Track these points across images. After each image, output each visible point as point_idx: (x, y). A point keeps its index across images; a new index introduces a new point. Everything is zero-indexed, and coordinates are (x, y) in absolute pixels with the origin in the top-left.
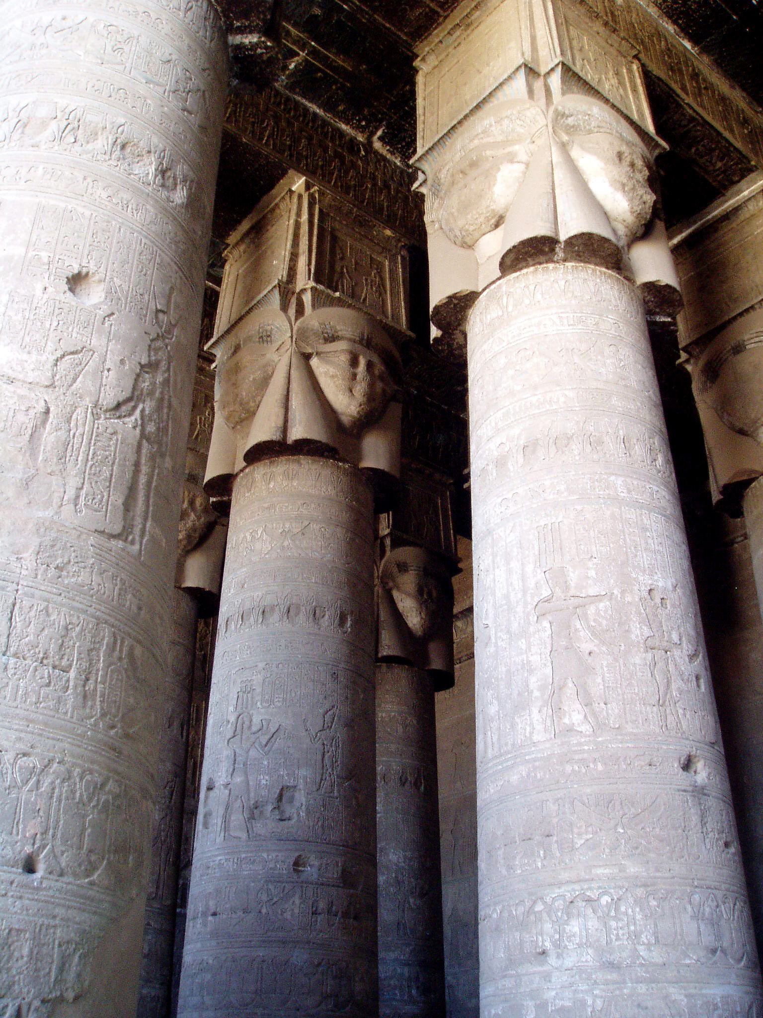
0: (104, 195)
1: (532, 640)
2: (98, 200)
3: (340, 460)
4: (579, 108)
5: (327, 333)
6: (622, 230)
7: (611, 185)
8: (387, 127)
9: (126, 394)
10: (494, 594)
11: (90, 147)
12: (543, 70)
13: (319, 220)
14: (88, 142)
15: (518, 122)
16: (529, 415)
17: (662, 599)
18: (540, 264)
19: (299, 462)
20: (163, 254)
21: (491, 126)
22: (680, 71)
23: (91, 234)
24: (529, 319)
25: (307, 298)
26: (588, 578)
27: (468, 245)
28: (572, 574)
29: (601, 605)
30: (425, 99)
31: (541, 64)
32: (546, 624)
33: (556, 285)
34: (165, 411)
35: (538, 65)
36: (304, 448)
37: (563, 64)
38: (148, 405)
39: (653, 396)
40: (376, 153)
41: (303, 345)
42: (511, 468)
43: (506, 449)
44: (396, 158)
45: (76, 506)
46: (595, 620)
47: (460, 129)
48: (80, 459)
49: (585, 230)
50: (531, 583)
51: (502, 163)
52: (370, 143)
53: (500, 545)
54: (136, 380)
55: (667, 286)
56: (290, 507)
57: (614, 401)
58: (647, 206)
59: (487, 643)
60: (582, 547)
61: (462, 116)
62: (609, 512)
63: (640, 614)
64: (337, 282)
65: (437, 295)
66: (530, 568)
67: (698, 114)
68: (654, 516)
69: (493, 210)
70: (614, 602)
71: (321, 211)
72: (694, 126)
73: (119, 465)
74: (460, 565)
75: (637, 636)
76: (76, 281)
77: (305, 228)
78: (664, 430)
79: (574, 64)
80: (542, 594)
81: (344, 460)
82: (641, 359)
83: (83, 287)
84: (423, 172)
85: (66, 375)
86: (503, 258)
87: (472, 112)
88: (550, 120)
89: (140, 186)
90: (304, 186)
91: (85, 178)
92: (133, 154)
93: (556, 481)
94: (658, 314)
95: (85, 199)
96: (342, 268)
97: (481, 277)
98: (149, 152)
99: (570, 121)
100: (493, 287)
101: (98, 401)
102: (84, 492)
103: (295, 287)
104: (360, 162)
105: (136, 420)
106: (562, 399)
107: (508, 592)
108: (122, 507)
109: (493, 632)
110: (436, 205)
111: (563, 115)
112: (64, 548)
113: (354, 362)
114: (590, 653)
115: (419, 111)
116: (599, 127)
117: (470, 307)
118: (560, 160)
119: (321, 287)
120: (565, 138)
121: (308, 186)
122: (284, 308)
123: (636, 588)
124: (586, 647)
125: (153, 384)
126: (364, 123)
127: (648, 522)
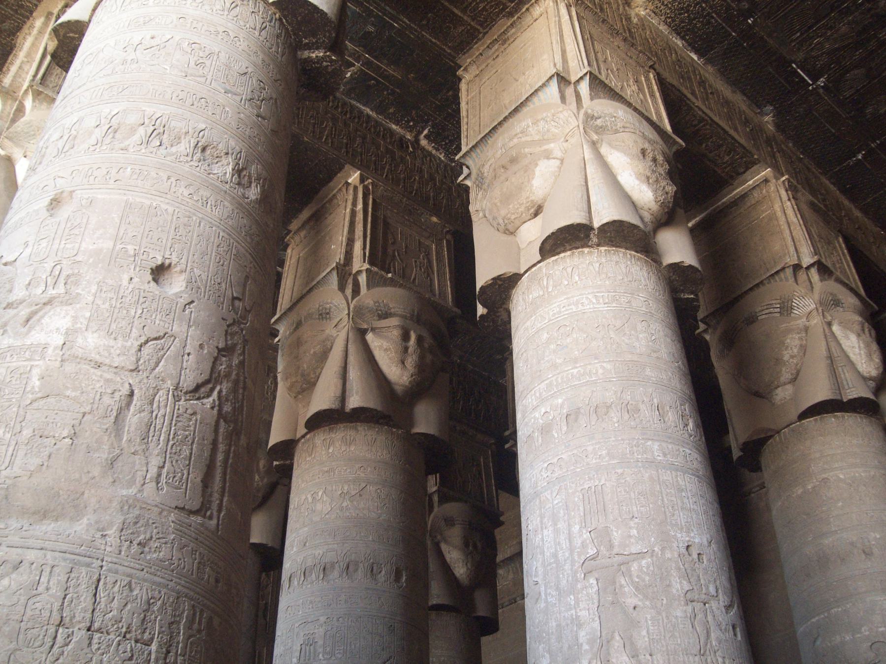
0: (186, 193)
1: (580, 596)
2: (181, 197)
3: (394, 426)
4: (606, 112)
5: (381, 310)
6: (648, 217)
7: (637, 179)
8: (433, 127)
9: (205, 376)
10: (543, 553)
11: (174, 149)
12: (573, 79)
13: (372, 209)
14: (172, 146)
15: (552, 122)
16: (571, 386)
17: (699, 554)
18: (577, 248)
19: (356, 429)
20: (239, 246)
21: (528, 127)
22: (689, 78)
23: (173, 228)
24: (568, 298)
25: (363, 279)
26: (630, 536)
28: (615, 533)
29: (644, 562)
30: (468, 104)
31: (571, 73)
32: (593, 581)
33: (591, 268)
34: (241, 391)
35: (569, 75)
36: (360, 416)
37: (591, 73)
38: (225, 387)
39: (682, 366)
40: (423, 149)
41: (359, 321)
42: (556, 435)
43: (551, 418)
44: (441, 154)
45: (158, 483)
46: (638, 577)
47: (500, 130)
48: (162, 439)
49: (616, 218)
50: (578, 542)
51: (539, 159)
52: (417, 141)
53: (547, 507)
54: (214, 363)
55: (690, 266)
56: (348, 470)
57: (648, 372)
58: (669, 195)
59: (537, 599)
60: (624, 508)
61: (502, 118)
62: (647, 475)
63: (679, 569)
64: (390, 264)
65: (483, 276)
66: (576, 528)
68: (687, 477)
69: (532, 201)
70: (655, 559)
71: (374, 200)
72: (704, 125)
73: (198, 444)
74: (501, 518)
75: (678, 591)
76: (159, 272)
77: (360, 217)
78: (693, 397)
79: (600, 73)
80: (588, 553)
81: (398, 427)
82: (669, 332)
83: (166, 277)
84: (468, 167)
85: (149, 360)
89: (218, 184)
90: (359, 178)
91: (169, 178)
92: (213, 156)
93: (597, 446)
94: (683, 291)
95: (168, 196)
96: (394, 251)
97: (522, 260)
98: (227, 154)
99: (599, 122)
100: (533, 269)
101: (179, 383)
102: (165, 471)
103: (351, 269)
104: (408, 157)
105: (214, 400)
106: (600, 371)
107: (556, 550)
108: (201, 484)
109: (543, 589)
111: (593, 117)
112: (147, 525)
113: (405, 337)
114: (635, 608)
115: (463, 113)
116: (624, 127)
117: (514, 287)
118: (592, 156)
119: (375, 269)
120: (595, 137)
121: (362, 179)
122: (342, 288)
123: (675, 545)
124: (631, 601)
125: (230, 366)
126: (411, 124)
127: (683, 483)
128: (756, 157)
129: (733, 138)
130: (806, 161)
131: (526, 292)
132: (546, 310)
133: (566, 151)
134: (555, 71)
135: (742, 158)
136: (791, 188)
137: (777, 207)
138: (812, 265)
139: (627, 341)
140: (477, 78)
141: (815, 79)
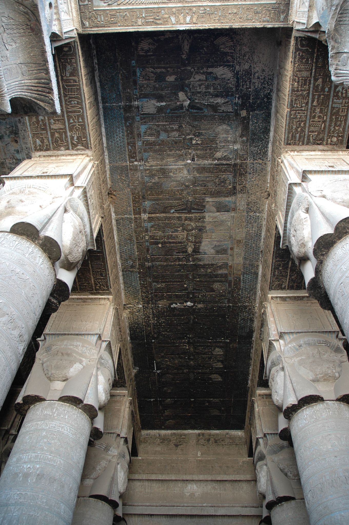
7: (103, 390)
12: (103, 339)
18: (72, 405)
21: (79, 346)
24: (60, 423)
27: (50, 379)
33: (73, 416)
37: (110, 342)
47: (67, 336)
49: (93, 405)
67: (122, 363)
69: (66, 375)
84: (45, 338)
86: (63, 397)
87: (74, 334)
88: (98, 358)
100: (52, 402)
110: (44, 354)
128: (126, 385)
129: (124, 375)
130: (136, 391)
131: (45, 409)
132: (50, 422)
133: (87, 365)
134: (99, 333)
135: (122, 383)
136: (131, 403)
137: (123, 408)
138: (124, 438)
139: (72, 454)
140: (66, 306)
141: (157, 370)
